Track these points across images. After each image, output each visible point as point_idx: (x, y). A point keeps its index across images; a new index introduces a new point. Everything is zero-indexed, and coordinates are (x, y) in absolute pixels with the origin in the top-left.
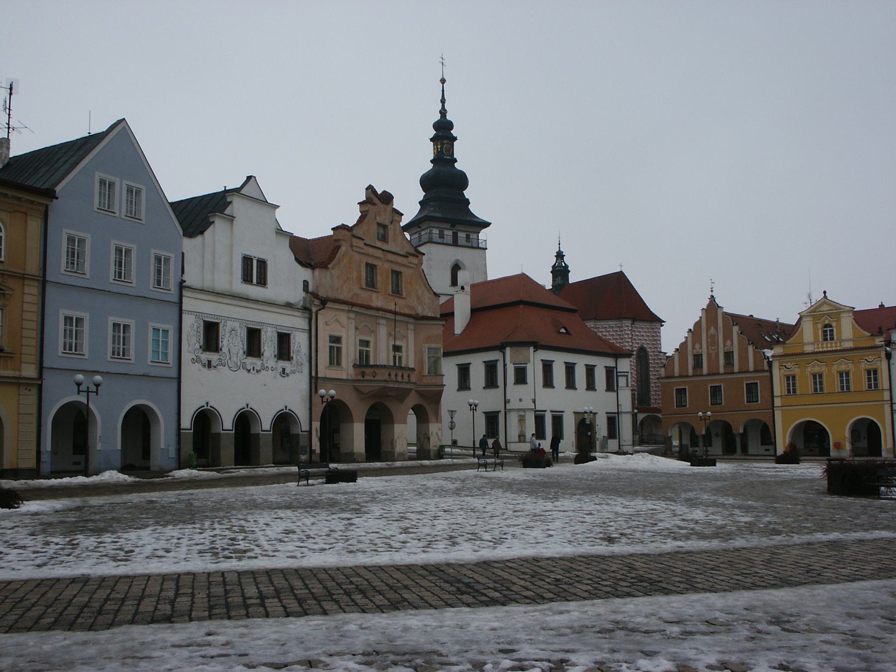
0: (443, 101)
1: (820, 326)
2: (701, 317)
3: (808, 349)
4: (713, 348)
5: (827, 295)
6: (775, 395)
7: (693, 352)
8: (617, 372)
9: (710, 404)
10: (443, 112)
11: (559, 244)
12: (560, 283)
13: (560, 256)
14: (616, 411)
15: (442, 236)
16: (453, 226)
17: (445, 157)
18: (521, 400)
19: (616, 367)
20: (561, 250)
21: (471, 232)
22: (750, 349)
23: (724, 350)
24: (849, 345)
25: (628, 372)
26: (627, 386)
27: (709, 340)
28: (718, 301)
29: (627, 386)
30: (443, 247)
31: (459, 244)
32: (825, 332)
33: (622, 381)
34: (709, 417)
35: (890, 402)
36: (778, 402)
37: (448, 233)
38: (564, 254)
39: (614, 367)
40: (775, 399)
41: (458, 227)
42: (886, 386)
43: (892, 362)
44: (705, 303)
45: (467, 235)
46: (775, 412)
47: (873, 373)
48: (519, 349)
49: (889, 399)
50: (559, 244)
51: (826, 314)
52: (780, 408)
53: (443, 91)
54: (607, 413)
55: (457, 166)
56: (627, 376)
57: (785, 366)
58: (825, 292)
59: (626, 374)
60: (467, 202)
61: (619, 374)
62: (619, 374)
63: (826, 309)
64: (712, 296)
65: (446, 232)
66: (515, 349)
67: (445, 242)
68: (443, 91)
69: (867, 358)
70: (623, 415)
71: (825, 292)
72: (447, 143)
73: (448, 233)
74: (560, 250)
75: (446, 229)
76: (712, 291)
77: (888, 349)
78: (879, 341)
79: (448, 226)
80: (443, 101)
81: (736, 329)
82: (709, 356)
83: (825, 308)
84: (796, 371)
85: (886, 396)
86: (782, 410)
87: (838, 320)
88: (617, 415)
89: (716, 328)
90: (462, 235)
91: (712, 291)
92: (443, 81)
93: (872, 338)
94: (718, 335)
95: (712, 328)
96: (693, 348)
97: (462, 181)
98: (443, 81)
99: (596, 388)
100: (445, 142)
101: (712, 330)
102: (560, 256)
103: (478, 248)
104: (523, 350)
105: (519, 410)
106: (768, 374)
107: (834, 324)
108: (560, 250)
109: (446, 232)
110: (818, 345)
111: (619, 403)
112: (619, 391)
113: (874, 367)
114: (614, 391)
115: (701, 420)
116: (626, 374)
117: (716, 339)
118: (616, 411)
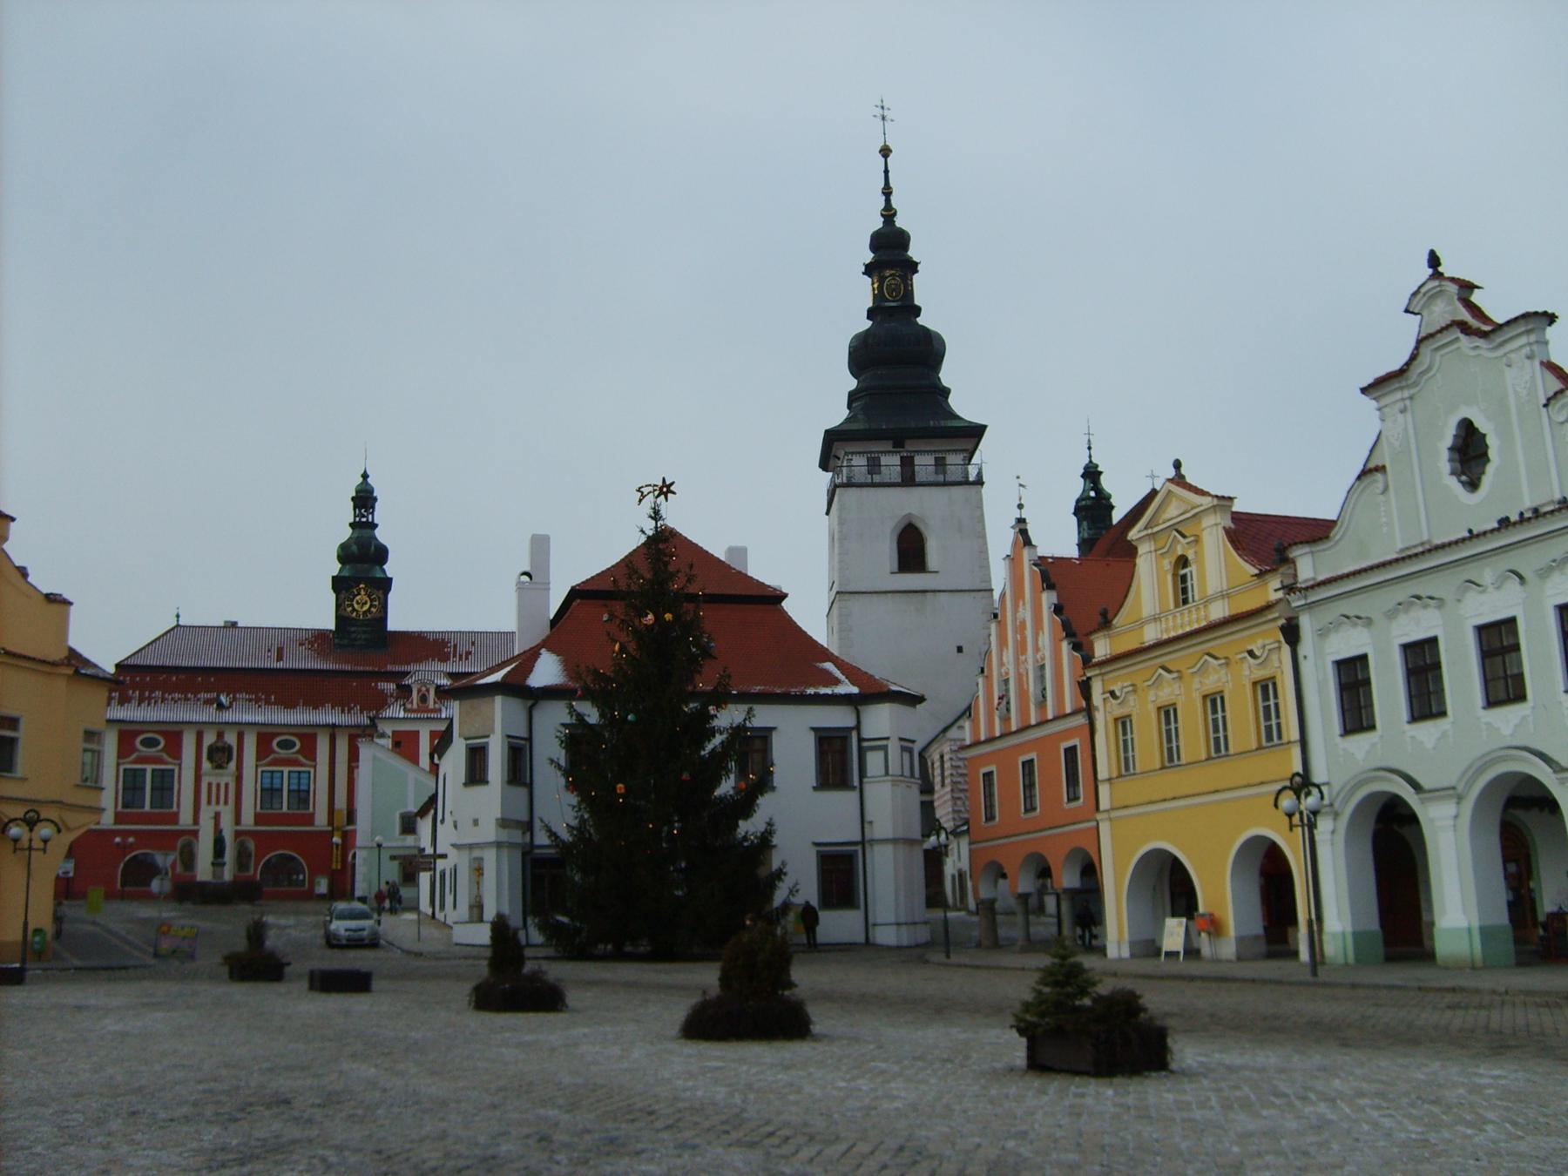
0: (887, 192)
3: (1151, 634)
5: (1183, 471)
6: (1100, 777)
8: (860, 740)
10: (889, 214)
11: (1089, 448)
12: (1086, 536)
13: (1091, 474)
14: (858, 838)
15: (874, 466)
16: (899, 444)
17: (887, 304)
18: (476, 822)
19: (858, 727)
20: (1094, 461)
21: (949, 451)
24: (1218, 611)
25: (887, 738)
26: (887, 773)
29: (887, 773)
30: (872, 490)
31: (917, 480)
33: (874, 761)
37: (891, 464)
38: (1099, 469)
39: (849, 729)
41: (910, 446)
42: (1293, 733)
43: (1302, 651)
45: (936, 458)
46: (1100, 824)
47: (1266, 688)
48: (475, 702)
50: (1089, 448)
53: (886, 172)
54: (817, 844)
55: (920, 321)
56: (885, 748)
59: (884, 743)
60: (946, 392)
61: (865, 744)
62: (865, 744)
64: (1021, 521)
65: (885, 460)
66: (468, 703)
67: (877, 479)
68: (886, 172)
70: (877, 848)
71: (1177, 465)
72: (891, 275)
73: (891, 464)
74: (1091, 461)
75: (882, 452)
76: (1020, 506)
78: (1272, 589)
79: (888, 446)
80: (887, 192)
81: (1048, 599)
84: (1132, 706)
86: (1110, 819)
88: (859, 848)
90: (924, 464)
91: (1020, 506)
92: (885, 152)
97: (929, 350)
98: (885, 152)
99: (775, 784)
100: (887, 273)
102: (1091, 474)
103: (965, 482)
104: (481, 704)
105: (471, 847)
106: (1081, 720)
108: (1091, 461)
109: (885, 460)
111: (868, 818)
112: (868, 788)
114: (854, 788)
116: (884, 742)
118: (858, 838)
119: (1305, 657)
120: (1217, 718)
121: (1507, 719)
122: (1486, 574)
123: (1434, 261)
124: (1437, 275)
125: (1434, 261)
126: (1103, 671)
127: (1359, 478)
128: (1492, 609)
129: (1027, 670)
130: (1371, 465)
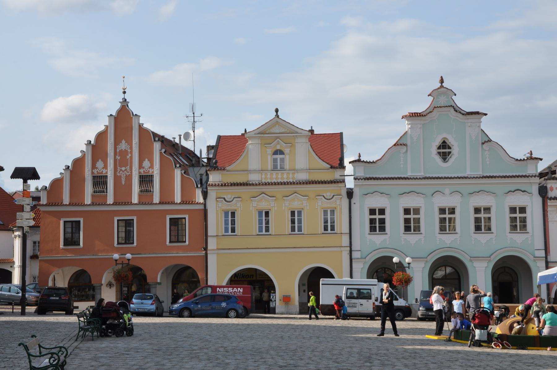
1: (270, 151)
2: (107, 127)
3: (254, 178)
4: (123, 169)
5: (279, 113)
6: (209, 235)
7: (92, 173)
9: (116, 242)
22: (178, 173)
23: (140, 173)
24: (303, 176)
27: (118, 158)
28: (133, 107)
32: (275, 160)
34: (129, 260)
35: (349, 249)
36: (212, 244)
40: (209, 239)
43: (353, 201)
44: (114, 109)
49: (348, 245)
51: (278, 137)
52: (217, 252)
57: (224, 199)
58: (277, 111)
63: (278, 131)
69: (325, 195)
71: (277, 111)
76: (124, 93)
77: (223, 185)
82: (117, 179)
83: (277, 129)
85: (345, 240)
86: (217, 254)
87: (292, 146)
89: (130, 143)
91: (124, 93)
93: (331, 170)
94: (131, 152)
95: (123, 142)
96: (94, 166)
101: (123, 145)
107: (287, 151)
110: (266, 174)
113: (333, 206)
115: (116, 264)
117: (128, 157)
119: (355, 203)
120: (294, 219)
121: (448, 239)
122: (447, 191)
123: (442, 81)
124: (442, 86)
125: (442, 81)
126: (220, 189)
127: (395, 145)
128: (447, 202)
129: (129, 178)
130: (401, 142)
